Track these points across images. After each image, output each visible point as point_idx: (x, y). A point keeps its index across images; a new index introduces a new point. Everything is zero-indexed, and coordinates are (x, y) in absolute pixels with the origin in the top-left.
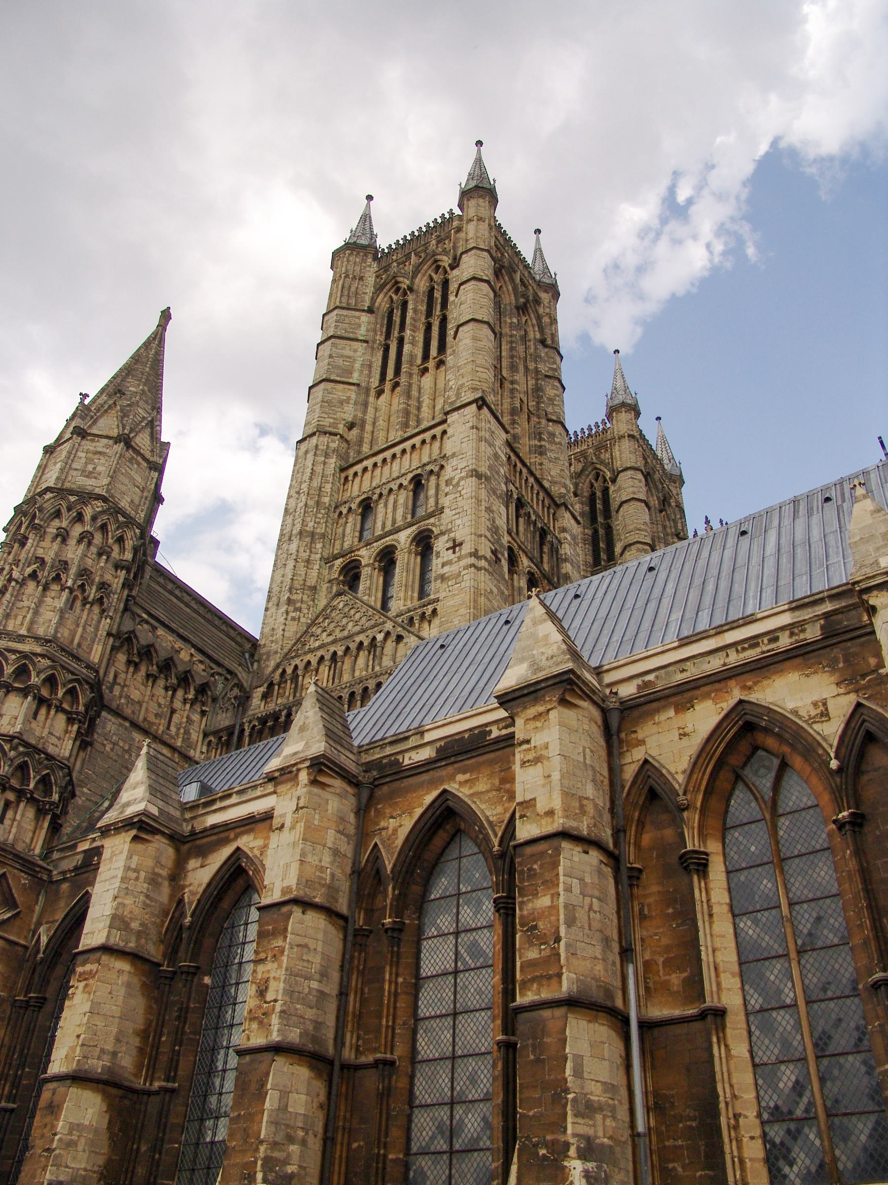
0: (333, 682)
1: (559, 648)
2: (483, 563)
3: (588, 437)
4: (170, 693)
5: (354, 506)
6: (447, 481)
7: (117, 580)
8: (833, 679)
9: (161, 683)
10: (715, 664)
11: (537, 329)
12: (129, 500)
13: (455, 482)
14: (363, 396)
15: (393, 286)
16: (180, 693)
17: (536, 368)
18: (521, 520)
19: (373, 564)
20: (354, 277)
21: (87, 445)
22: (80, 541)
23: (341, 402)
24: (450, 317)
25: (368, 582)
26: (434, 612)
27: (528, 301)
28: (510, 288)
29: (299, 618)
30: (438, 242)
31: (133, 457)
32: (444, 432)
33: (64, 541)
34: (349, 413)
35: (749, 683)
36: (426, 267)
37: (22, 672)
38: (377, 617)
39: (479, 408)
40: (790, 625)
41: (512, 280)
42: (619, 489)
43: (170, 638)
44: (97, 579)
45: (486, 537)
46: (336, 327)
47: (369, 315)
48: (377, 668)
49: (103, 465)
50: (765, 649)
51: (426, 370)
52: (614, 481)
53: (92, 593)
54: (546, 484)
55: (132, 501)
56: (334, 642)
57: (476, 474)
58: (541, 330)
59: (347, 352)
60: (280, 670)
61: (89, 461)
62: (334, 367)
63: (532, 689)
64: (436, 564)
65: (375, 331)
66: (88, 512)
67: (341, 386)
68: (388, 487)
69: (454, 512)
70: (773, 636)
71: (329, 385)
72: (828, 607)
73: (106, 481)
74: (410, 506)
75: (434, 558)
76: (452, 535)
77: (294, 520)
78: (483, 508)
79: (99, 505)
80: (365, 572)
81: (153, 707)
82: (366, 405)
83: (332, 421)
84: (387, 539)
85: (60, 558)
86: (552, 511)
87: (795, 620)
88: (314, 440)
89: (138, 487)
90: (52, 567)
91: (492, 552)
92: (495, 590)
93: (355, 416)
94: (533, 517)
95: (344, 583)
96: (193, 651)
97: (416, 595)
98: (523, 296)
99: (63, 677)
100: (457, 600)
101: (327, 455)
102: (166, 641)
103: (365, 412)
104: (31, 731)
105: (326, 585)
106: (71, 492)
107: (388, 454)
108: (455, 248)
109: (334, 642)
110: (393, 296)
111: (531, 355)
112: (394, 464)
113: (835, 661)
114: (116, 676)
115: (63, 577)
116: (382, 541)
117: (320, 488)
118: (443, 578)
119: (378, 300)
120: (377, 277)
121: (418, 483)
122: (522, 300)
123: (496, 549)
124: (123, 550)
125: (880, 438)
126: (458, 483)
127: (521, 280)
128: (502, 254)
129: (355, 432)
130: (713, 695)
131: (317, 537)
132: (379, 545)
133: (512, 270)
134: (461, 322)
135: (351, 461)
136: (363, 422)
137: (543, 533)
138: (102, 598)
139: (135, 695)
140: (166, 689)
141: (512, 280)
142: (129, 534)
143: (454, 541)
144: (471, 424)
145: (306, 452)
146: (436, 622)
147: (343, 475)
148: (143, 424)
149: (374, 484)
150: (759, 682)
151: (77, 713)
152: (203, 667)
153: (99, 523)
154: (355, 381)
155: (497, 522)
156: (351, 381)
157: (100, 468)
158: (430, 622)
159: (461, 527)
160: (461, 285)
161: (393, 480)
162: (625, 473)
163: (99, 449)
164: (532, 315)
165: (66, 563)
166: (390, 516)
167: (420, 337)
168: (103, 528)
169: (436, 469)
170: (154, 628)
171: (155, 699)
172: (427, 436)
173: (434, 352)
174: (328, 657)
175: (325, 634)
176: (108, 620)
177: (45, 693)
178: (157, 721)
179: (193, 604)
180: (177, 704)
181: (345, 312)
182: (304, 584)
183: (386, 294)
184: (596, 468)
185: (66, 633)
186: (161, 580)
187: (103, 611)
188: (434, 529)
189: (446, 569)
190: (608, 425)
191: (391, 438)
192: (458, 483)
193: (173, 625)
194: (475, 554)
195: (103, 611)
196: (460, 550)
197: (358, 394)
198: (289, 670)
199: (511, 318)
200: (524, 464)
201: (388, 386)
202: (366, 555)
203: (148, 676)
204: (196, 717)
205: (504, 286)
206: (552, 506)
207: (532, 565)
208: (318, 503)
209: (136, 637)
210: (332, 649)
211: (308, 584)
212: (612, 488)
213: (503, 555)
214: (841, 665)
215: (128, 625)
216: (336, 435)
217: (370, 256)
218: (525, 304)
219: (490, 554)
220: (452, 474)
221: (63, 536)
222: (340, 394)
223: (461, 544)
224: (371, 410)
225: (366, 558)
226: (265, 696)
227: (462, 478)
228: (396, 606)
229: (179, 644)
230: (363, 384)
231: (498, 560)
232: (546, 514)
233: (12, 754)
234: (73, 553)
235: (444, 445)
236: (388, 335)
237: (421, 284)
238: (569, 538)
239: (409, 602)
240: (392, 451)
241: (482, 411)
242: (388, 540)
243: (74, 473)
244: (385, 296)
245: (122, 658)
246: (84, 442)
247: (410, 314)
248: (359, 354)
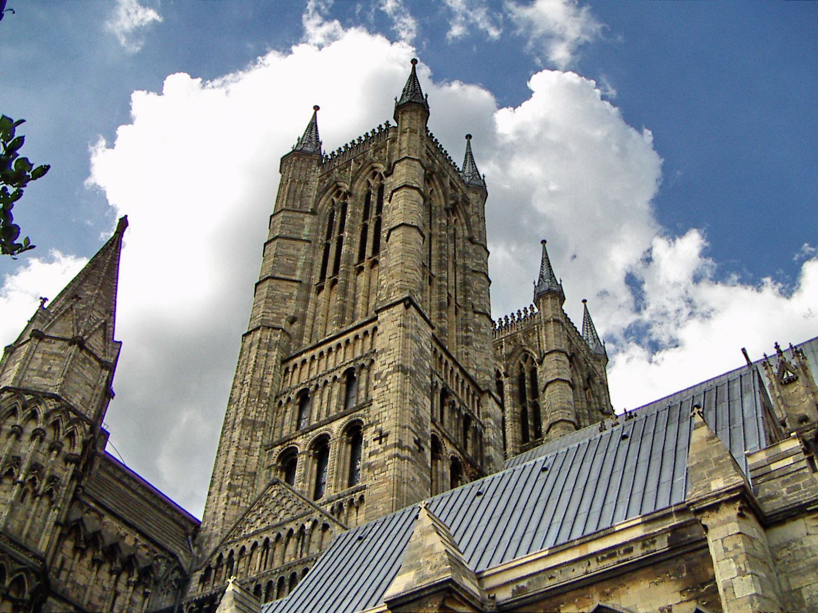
0: (265, 568)
1: (442, 558)
2: (406, 453)
3: (517, 322)
4: (114, 576)
5: (293, 397)
6: (376, 375)
7: (65, 473)
8: (677, 587)
9: (106, 567)
10: (578, 572)
12: (81, 397)
13: (383, 376)
14: (305, 292)
15: (334, 190)
16: (124, 577)
17: (465, 264)
18: (446, 409)
19: (308, 452)
20: (300, 182)
21: (43, 346)
22: (33, 438)
23: (284, 299)
24: (384, 220)
25: (303, 469)
26: (362, 499)
27: (457, 202)
28: (440, 191)
29: (239, 503)
30: (375, 151)
31: (86, 358)
32: (375, 329)
34: (291, 308)
35: (608, 590)
38: (306, 507)
39: (407, 307)
40: (642, 537)
41: (442, 184)
42: (546, 370)
44: (47, 473)
45: (409, 428)
46: (282, 228)
47: (312, 216)
48: (305, 555)
49: (58, 365)
50: (621, 559)
51: (361, 269)
52: (541, 362)
53: (43, 486)
54: (472, 373)
55: (83, 398)
56: (267, 529)
57: (402, 369)
58: (470, 229)
59: (291, 251)
60: (218, 555)
61: (45, 361)
62: (280, 265)
63: (417, 596)
64: (364, 452)
65: (317, 231)
66: (42, 410)
67: (286, 283)
68: (323, 379)
69: (381, 405)
70: (627, 547)
71: (274, 282)
72: (675, 521)
73: (59, 381)
74: (343, 398)
75: (363, 447)
76: (379, 426)
77: (237, 409)
78: (408, 401)
79: (51, 404)
80: (301, 459)
81: (98, 591)
82: (307, 300)
83: (275, 315)
84: (321, 428)
85: (13, 454)
86: (476, 398)
87: (647, 533)
88: (258, 334)
89: (90, 386)
90: (6, 462)
91: (415, 441)
92: (417, 478)
94: (458, 406)
95: (282, 469)
96: (137, 536)
97: (346, 482)
98: (452, 198)
100: (382, 488)
101: (269, 349)
102: (112, 527)
103: (306, 307)
105: (265, 471)
106: (27, 392)
107: (324, 348)
108: (390, 157)
109: (267, 529)
110: (334, 199)
111: (460, 252)
112: (330, 358)
113: (680, 571)
114: (63, 562)
115: (15, 471)
116: (317, 430)
117: (263, 379)
118: (370, 467)
119: (321, 203)
120: (321, 181)
121: (350, 377)
122: (452, 202)
123: (419, 439)
124: (73, 444)
125: (744, 350)
126: (386, 377)
127: (451, 183)
128: (433, 162)
129: (296, 325)
130: (577, 600)
131: (258, 425)
132: (314, 434)
133: (442, 175)
134: (392, 227)
135: (292, 353)
136: (304, 316)
137: (467, 419)
138: (51, 490)
139: (81, 580)
140: (111, 573)
141: (442, 184)
142: (79, 430)
143: (381, 432)
144: (398, 322)
145: (251, 345)
146: (363, 508)
147: (284, 367)
148: (97, 326)
149: (312, 376)
150: (615, 589)
151: (23, 601)
152: (146, 551)
153: (51, 420)
154: (297, 278)
155: (420, 413)
156: (294, 278)
158: (357, 508)
159: (387, 419)
160: (393, 191)
161: (328, 373)
162: (551, 355)
163: (55, 351)
164: (461, 215)
165: (19, 458)
166: (325, 406)
167: (357, 238)
168: (56, 425)
169: (367, 363)
170: (101, 516)
171: (99, 583)
172: (360, 332)
173: (369, 252)
174: (260, 543)
175: (259, 521)
176: (56, 512)
178: (101, 604)
179: (140, 491)
180: (121, 587)
181: (290, 214)
182: (245, 471)
183: (328, 197)
184: (524, 351)
186: (110, 469)
187: (52, 503)
188: (363, 420)
189: (373, 458)
190: (536, 310)
191: (329, 332)
192: (386, 377)
193: (120, 512)
194: (399, 445)
196: (386, 441)
197: (300, 291)
198: (226, 555)
199: (440, 220)
200: (449, 356)
201: (327, 283)
202: (302, 443)
203: (94, 561)
204: (138, 599)
205: (435, 190)
206: (477, 393)
207: (455, 450)
208: (260, 393)
209: (84, 525)
210: (265, 536)
211: (249, 470)
212: (539, 370)
213: (426, 444)
214: (684, 574)
215: (76, 514)
216: (278, 329)
217: (315, 162)
218: (454, 205)
219: (413, 443)
220: (381, 369)
222: (283, 290)
223: (386, 435)
224: (311, 305)
225: (302, 446)
226: (204, 580)
227: (389, 373)
228: (328, 492)
230: (305, 282)
231: (421, 449)
232: (470, 401)
234: (27, 448)
235: (374, 341)
236: (329, 236)
237: (360, 189)
238: (492, 423)
239: (339, 489)
240: (329, 345)
241: (409, 310)
242: (322, 430)
243: (31, 373)
244: (327, 199)
245: (69, 544)
246: (42, 344)
247: (349, 216)
248: (302, 253)
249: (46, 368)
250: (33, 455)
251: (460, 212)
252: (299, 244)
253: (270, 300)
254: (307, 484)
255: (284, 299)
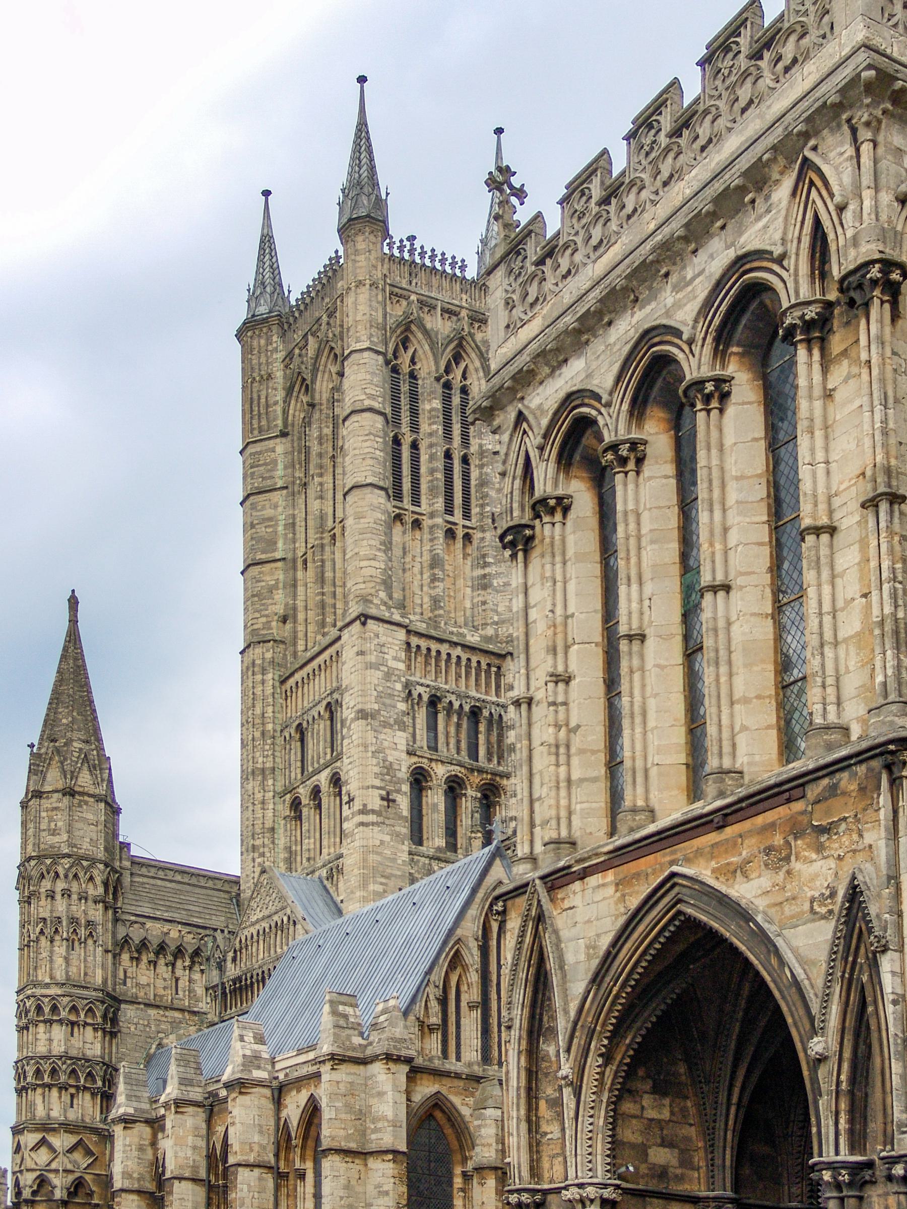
7: (97, 913)
11: (481, 374)
21: (46, 803)
31: (81, 801)
33: (53, 898)
36: (324, 359)
37: (54, 1009)
43: (158, 925)
53: (83, 932)
73: (65, 837)
81: (160, 983)
93: (286, 605)
96: (180, 927)
99: (80, 1004)
101: (264, 671)
102: (155, 930)
104: (73, 1046)
106: (46, 857)
114: (125, 972)
115: (60, 929)
124: (95, 886)
129: (289, 626)
142: (95, 872)
153: (71, 876)
157: (60, 824)
163: (55, 805)
168: (76, 876)
177: (73, 1018)
185: (75, 970)
186: (144, 871)
187: (95, 942)
195: (95, 942)
208: (263, 734)
221: (51, 895)
229: (167, 927)
233: (64, 1067)
234: (61, 906)
243: (44, 834)
245: (125, 957)
246: (43, 801)
249: (53, 825)
250: (68, 910)
251: (469, 350)
252: (278, 497)
253: (256, 599)
254: (312, 840)
255: (271, 590)
